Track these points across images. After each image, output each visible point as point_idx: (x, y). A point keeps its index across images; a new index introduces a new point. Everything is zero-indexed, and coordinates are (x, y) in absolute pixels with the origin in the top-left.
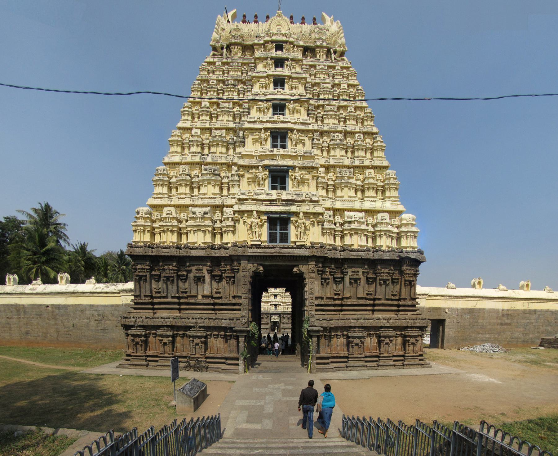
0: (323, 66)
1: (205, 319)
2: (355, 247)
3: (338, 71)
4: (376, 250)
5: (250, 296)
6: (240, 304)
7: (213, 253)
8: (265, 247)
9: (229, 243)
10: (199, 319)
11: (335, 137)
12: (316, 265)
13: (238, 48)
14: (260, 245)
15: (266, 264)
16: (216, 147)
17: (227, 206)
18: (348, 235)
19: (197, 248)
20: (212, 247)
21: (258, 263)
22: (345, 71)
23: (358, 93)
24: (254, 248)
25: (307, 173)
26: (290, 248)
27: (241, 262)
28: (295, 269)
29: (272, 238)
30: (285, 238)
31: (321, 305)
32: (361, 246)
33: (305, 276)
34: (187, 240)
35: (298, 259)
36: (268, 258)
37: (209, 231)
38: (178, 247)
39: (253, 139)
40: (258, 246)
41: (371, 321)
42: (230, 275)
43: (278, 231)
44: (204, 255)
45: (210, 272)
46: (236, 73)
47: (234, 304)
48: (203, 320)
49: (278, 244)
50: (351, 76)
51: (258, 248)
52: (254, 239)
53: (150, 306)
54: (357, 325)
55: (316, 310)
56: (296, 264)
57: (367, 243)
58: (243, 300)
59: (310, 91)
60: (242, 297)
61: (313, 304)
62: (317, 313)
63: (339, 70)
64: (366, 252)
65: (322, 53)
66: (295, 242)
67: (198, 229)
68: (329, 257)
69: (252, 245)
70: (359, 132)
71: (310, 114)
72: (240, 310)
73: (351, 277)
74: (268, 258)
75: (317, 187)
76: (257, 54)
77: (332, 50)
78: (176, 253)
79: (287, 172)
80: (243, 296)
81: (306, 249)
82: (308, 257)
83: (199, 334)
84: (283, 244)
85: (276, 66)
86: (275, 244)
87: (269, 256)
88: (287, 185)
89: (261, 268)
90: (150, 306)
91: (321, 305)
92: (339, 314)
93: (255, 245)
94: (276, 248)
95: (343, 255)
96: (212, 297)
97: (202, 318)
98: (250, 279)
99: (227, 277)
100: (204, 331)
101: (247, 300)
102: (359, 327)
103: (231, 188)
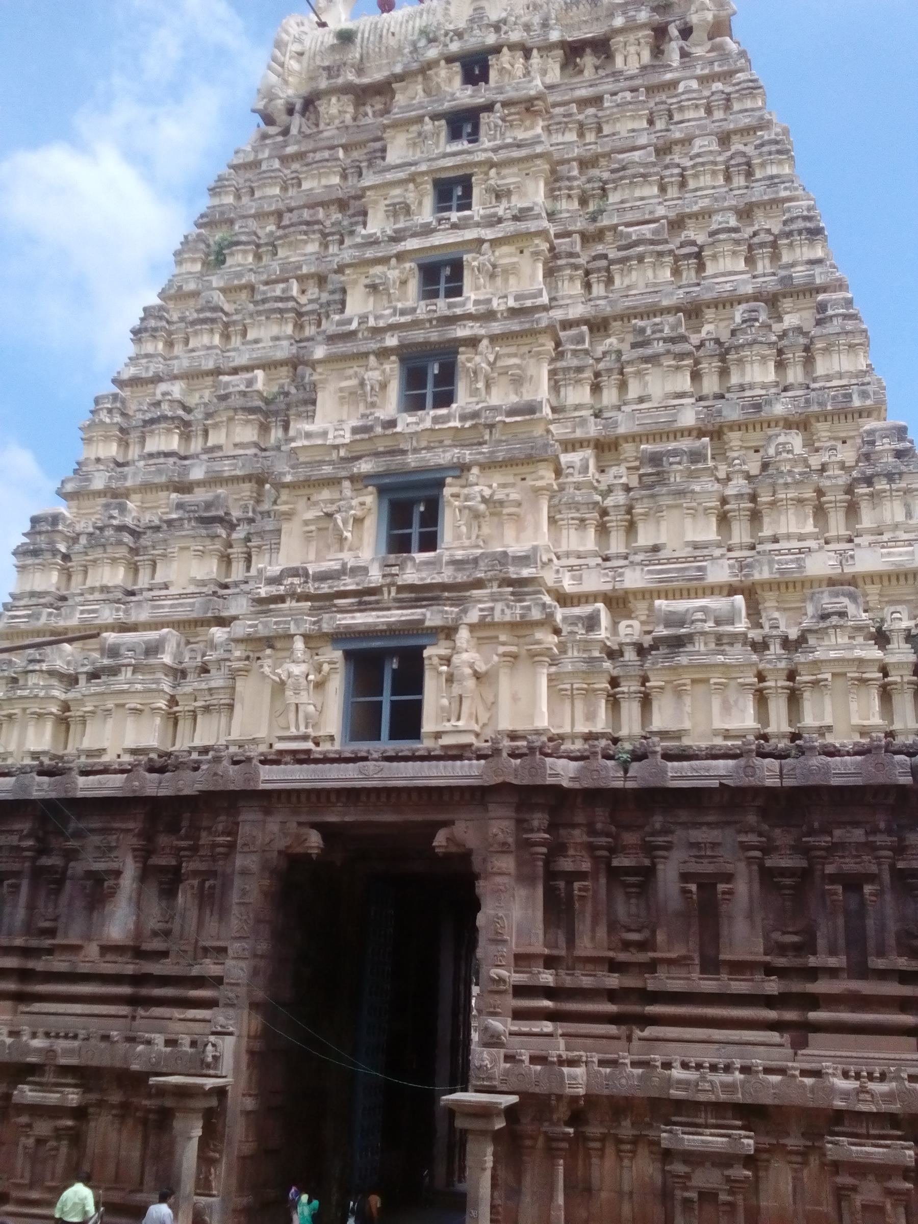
0: (628, 95)
2: (693, 742)
3: (683, 97)
5: (263, 947)
6: (218, 981)
8: (326, 760)
10: (66, 1037)
11: (649, 332)
12: (519, 822)
14: (308, 752)
15: (332, 818)
16: (224, 431)
21: (303, 818)
22: (717, 86)
23: (761, 154)
24: (286, 764)
25: (510, 479)
26: (422, 758)
27: (241, 818)
28: (440, 840)
32: (727, 735)
33: (477, 866)
35: (446, 797)
36: (333, 798)
39: (341, 390)
40: (303, 756)
41: (775, 1079)
43: (387, 699)
44: (119, 794)
45: (144, 854)
46: (324, 182)
47: (200, 981)
48: (76, 1044)
50: (739, 99)
51: (301, 762)
52: (293, 731)
54: (702, 1097)
55: (519, 1015)
58: (230, 963)
59: (570, 188)
60: (230, 952)
61: (502, 987)
62: (525, 1026)
63: (694, 91)
64: (742, 761)
65: (632, 49)
66: (438, 735)
67: (117, 706)
68: (576, 785)
69: (281, 752)
70: (746, 299)
71: (560, 268)
74: (333, 798)
79: (441, 484)
80: (235, 947)
81: (479, 757)
83: (53, 1098)
84: (405, 746)
85: (455, 134)
87: (339, 792)
88: (439, 529)
89: (314, 840)
93: (294, 752)
94: (365, 759)
96: (138, 953)
97: (75, 1037)
99: (195, 873)
100: (75, 1086)
101: (243, 964)
102: (718, 1108)
103: (254, 558)
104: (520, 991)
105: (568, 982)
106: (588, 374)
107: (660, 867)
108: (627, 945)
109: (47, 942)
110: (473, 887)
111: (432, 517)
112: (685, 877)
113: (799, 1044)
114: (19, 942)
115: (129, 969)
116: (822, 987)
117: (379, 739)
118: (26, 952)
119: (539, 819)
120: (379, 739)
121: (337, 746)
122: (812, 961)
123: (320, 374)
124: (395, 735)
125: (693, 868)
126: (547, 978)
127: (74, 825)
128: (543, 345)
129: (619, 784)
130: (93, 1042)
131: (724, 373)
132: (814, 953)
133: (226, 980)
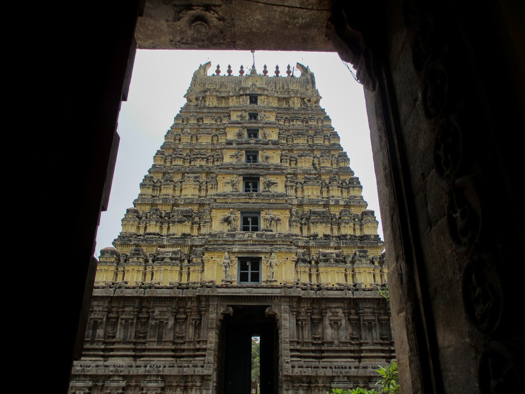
1: (165, 367)
4: (356, 287)
6: (205, 350)
7: (180, 293)
9: (197, 283)
12: (289, 306)
13: (213, 99)
17: (196, 246)
18: (324, 272)
19: (162, 288)
20: (180, 287)
29: (243, 277)
30: (256, 277)
31: (298, 351)
34: (152, 279)
37: (176, 271)
38: (142, 286)
42: (196, 318)
43: (250, 271)
47: (198, 350)
49: (250, 283)
53: (102, 353)
55: (292, 356)
56: (269, 304)
57: (346, 281)
72: (204, 356)
73: (330, 318)
75: (290, 226)
76: (231, 104)
77: (305, 100)
78: (140, 293)
82: (281, 297)
84: (254, 284)
86: (244, 284)
89: (231, 309)
90: (102, 353)
91: (298, 351)
92: (319, 362)
95: (319, 294)
98: (219, 323)
104: (291, 350)
105: (303, 348)
106: (294, 187)
107: (324, 318)
108: (315, 339)
109: (143, 341)
110: (276, 324)
111: (256, 221)
112: (330, 320)
113: (360, 362)
114: (135, 340)
115: (173, 347)
116: (363, 348)
117: (248, 281)
118: (135, 343)
119: (295, 304)
120: (248, 281)
121: (235, 284)
122: (362, 342)
123: (220, 178)
124: (252, 280)
125: (333, 318)
126: (298, 347)
127: (151, 305)
128: (283, 178)
129: (315, 296)
130: (167, 368)
131: (328, 191)
132: (361, 339)
133: (207, 349)
